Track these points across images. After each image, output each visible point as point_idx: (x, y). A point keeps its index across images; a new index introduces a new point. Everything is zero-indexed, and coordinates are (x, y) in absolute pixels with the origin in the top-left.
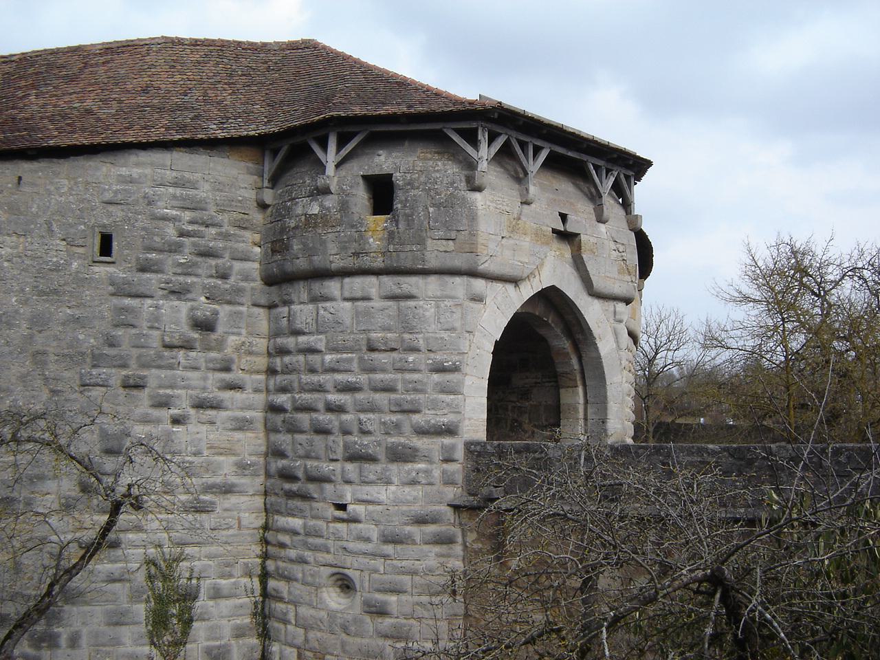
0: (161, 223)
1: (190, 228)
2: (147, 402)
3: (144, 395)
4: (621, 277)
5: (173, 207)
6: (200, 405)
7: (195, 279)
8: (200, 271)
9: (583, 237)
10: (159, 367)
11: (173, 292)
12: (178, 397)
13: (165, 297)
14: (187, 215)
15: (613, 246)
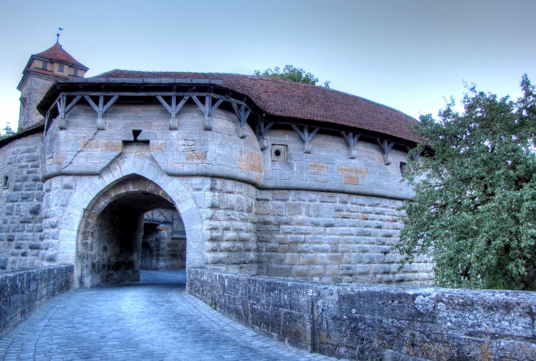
0: (21, 169)
1: (31, 169)
2: (14, 247)
3: (13, 244)
4: (189, 161)
5: (26, 162)
6: (32, 247)
7: (32, 192)
8: (33, 188)
9: (151, 142)
10: (18, 231)
11: (23, 199)
12: (24, 244)
13: (22, 201)
14: (30, 164)
15: (182, 142)
